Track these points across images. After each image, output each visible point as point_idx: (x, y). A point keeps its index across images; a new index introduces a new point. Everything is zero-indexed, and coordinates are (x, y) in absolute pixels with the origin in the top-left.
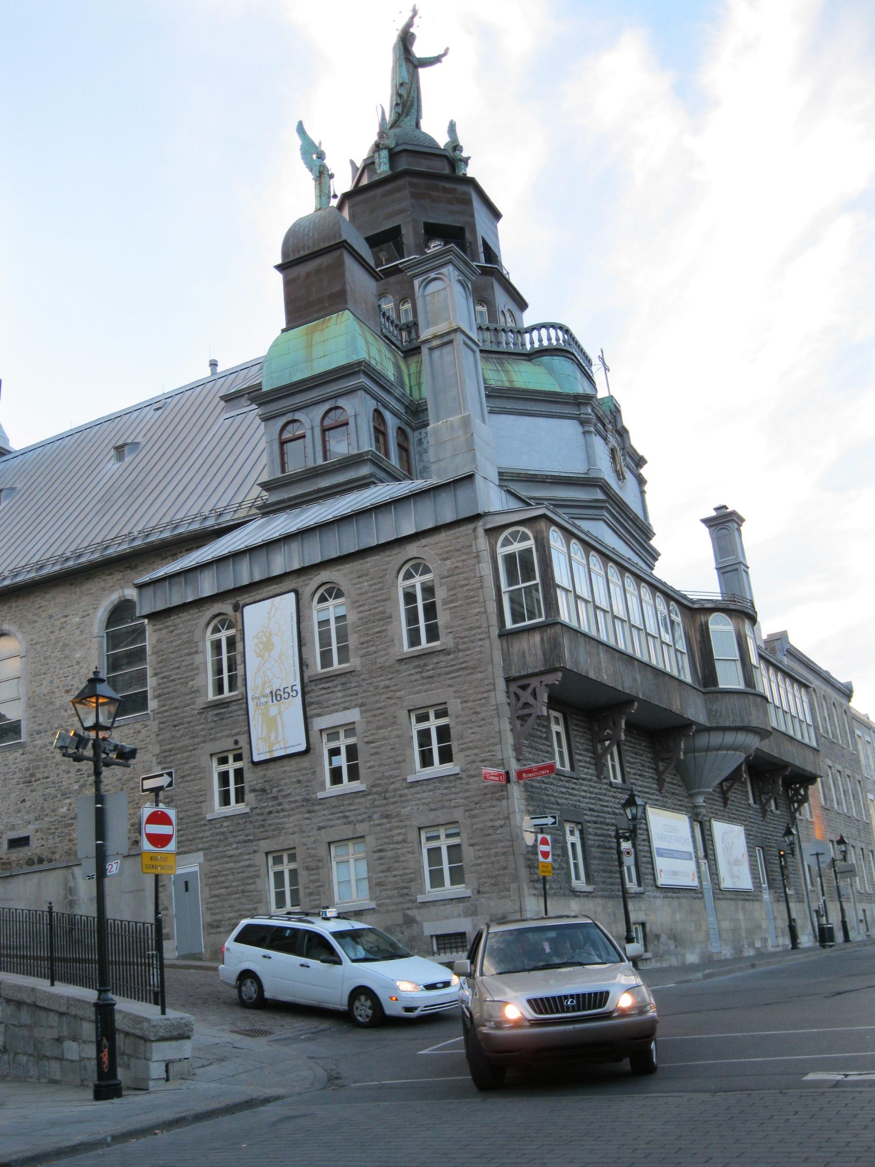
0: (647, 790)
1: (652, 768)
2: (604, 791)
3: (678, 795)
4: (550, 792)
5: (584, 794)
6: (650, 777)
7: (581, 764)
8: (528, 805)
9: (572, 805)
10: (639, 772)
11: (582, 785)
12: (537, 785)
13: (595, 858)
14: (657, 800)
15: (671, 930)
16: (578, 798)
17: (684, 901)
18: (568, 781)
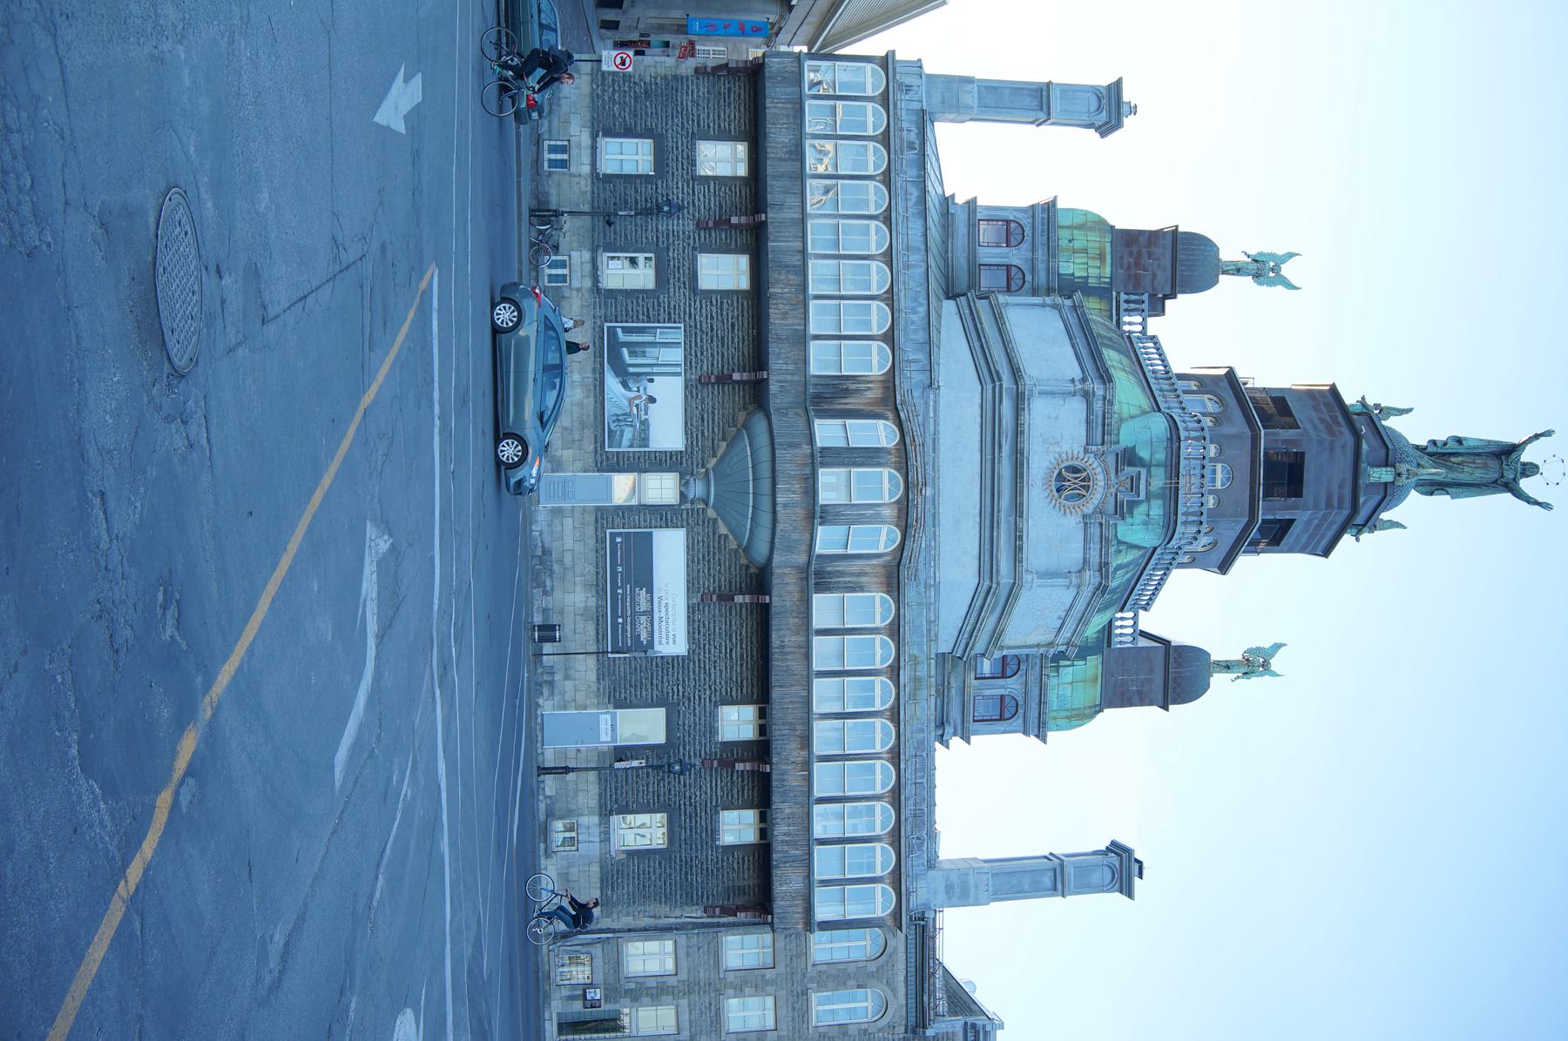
0: (699, 338)
1: (723, 366)
4: (676, 121)
5: (680, 185)
6: (712, 355)
9: (668, 159)
10: (715, 328)
11: (688, 187)
12: (679, 98)
13: (625, 188)
17: (592, 400)
18: (688, 156)
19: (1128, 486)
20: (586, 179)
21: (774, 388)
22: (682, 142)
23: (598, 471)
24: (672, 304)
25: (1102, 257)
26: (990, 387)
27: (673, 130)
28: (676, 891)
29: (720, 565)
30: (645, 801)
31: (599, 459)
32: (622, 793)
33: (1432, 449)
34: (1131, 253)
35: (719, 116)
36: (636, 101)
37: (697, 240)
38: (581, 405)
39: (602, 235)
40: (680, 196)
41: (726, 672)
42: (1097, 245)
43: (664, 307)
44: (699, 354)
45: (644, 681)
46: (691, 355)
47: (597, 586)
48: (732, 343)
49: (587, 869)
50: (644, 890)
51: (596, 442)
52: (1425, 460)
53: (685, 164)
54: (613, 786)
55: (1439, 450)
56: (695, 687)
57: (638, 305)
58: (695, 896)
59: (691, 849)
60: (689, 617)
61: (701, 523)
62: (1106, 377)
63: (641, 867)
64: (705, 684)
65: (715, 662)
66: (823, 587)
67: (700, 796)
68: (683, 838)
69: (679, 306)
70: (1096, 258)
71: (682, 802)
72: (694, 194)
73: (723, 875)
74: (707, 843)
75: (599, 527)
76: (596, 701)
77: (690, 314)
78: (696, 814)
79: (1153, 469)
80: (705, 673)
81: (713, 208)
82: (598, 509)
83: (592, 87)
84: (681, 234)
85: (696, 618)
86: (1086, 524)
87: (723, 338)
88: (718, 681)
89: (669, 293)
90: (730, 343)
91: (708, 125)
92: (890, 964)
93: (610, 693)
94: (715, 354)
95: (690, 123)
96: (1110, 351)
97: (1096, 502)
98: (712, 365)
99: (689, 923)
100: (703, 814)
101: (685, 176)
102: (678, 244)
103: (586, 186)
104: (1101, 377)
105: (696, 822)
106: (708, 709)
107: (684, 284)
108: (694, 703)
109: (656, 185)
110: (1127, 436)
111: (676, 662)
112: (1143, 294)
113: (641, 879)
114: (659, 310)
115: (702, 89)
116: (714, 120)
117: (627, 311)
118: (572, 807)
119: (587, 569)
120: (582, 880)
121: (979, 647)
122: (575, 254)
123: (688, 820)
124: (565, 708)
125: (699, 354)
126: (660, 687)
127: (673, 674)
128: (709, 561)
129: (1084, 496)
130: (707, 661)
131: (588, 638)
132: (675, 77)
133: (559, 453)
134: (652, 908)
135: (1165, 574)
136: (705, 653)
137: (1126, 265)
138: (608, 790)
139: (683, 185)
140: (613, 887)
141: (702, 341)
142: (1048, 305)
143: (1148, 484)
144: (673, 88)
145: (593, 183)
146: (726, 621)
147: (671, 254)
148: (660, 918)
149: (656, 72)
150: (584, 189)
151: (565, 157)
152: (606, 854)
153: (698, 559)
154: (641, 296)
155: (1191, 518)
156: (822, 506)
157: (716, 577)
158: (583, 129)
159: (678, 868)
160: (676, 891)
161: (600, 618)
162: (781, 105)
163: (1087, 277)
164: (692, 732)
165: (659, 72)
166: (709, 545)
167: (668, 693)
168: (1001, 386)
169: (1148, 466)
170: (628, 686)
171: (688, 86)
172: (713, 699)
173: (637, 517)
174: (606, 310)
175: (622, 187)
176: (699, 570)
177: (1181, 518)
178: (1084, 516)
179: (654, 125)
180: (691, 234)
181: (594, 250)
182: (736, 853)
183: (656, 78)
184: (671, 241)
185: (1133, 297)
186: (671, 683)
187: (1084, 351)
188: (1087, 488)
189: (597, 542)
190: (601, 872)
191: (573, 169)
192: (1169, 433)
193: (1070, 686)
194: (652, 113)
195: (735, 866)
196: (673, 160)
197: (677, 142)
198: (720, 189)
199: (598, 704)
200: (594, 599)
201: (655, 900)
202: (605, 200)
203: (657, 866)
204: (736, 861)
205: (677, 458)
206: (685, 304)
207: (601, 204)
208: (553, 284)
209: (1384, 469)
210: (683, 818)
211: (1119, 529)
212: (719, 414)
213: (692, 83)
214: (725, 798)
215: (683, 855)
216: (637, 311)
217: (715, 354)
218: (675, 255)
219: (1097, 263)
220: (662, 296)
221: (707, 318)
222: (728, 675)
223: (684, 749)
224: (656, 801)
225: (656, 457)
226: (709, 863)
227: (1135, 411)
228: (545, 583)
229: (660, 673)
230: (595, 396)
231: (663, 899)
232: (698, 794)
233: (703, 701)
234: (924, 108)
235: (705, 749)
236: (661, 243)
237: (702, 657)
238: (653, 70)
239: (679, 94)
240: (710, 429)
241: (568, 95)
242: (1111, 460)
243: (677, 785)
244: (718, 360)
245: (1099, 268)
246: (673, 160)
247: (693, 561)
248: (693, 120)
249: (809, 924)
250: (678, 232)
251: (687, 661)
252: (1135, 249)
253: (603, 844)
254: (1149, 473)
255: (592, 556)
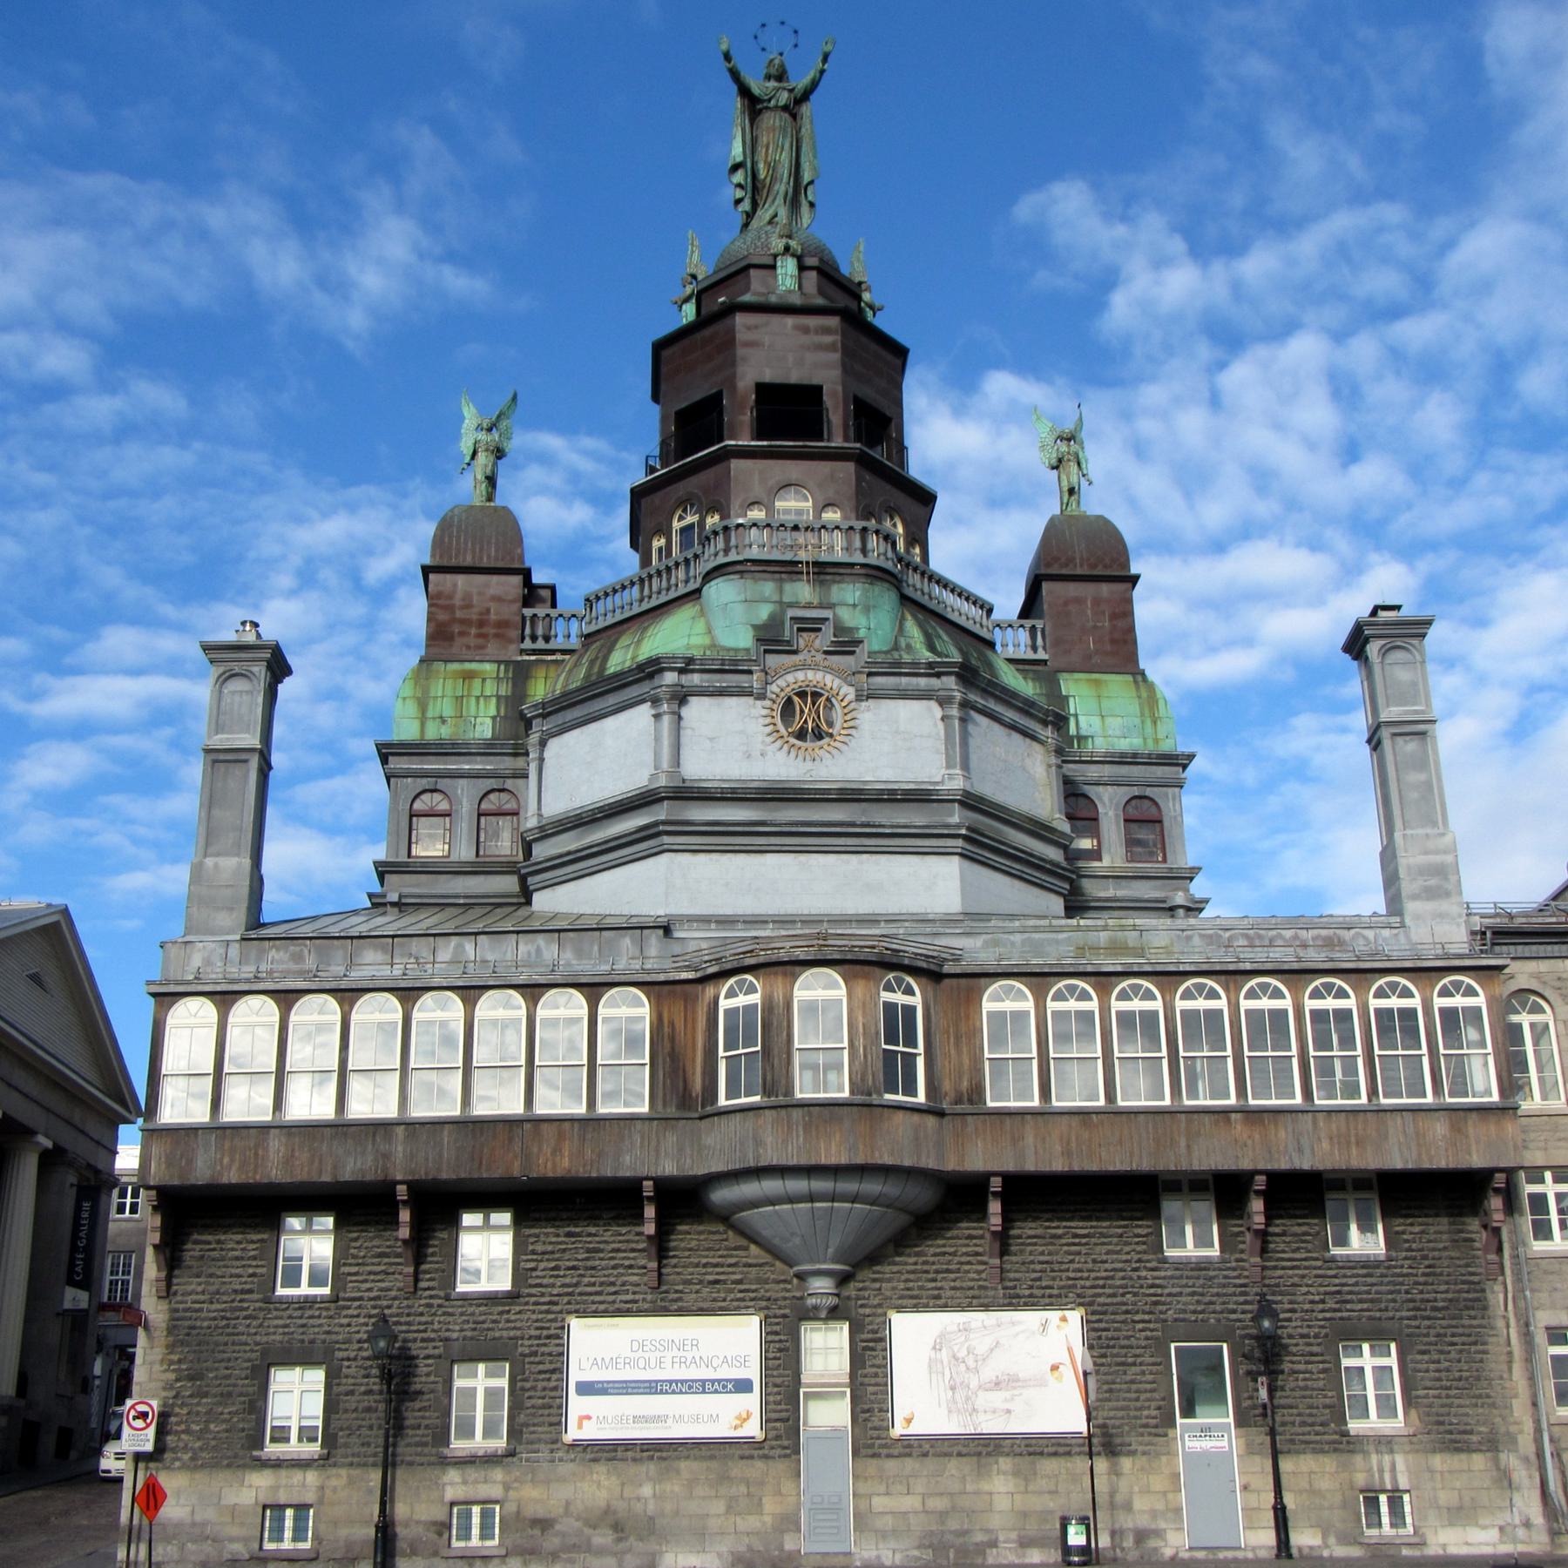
1: (633, 1250)
2: (421, 1309)
3: (740, 1282)
4: (241, 1329)
5: (345, 1321)
6: (614, 1267)
7: (354, 1278)
8: (171, 1353)
9: (302, 1341)
12: (206, 1324)
13: (346, 1411)
14: (636, 1302)
15: (607, 1511)
16: (326, 1328)
17: (683, 1465)
18: (300, 1308)
19: (813, 635)
20: (328, 1477)
21: (668, 1168)
22: (276, 1318)
23: (798, 1453)
24: (533, 1332)
25: (468, 676)
26: (666, 839)
27: (256, 1334)
28: (1463, 1326)
29: (944, 1254)
30: (1322, 1376)
31: (778, 1452)
32: (1311, 1415)
33: (746, 206)
34: (462, 634)
35: (237, 1258)
36: (206, 1395)
37: (432, 1293)
38: (692, 1483)
39: (419, 1449)
40: (362, 1320)
41: (1110, 1243)
42: (449, 683)
43: (538, 1345)
44: (613, 1289)
45: (1128, 1378)
46: (614, 1302)
47: (979, 1454)
48: (595, 1235)
49: (1438, 1476)
50: (1467, 1379)
51: (751, 1457)
52: (764, 215)
53: (310, 1313)
54: (1300, 1430)
55: (749, 195)
56: (1135, 1294)
57: (534, 1388)
58: (1471, 1296)
59: (1394, 1301)
60: (1026, 1304)
61: (877, 1285)
62: (650, 669)
63: (1429, 1384)
64: (1131, 1278)
65: (1094, 1261)
66: (977, 1093)
67: (1307, 1286)
68: (1378, 1314)
69: (537, 1321)
70: (470, 686)
71: (1320, 1316)
72: (360, 1299)
73: (1434, 1249)
74: (1382, 1276)
75: (884, 1451)
76: (1164, 1459)
77: (550, 1303)
78: (1339, 1292)
79: (786, 599)
80: (1112, 1278)
81: (383, 1268)
82: (855, 1453)
83: (179, 1468)
84: (423, 1319)
85: (1027, 1292)
86: (868, 697)
87: (589, 1251)
88: (1124, 1257)
89: (516, 1338)
90: (597, 1239)
91: (251, 1276)
92: (1558, 984)
93: (1150, 1434)
94: (612, 1263)
95: (246, 1305)
96: (609, 663)
97: (837, 682)
98: (631, 1267)
99: (1515, 1306)
100: (1337, 1281)
101: (331, 1313)
102: (439, 1322)
103: (339, 1476)
104: (651, 676)
105: (1350, 1293)
106: (1169, 1273)
107: (501, 1313)
108: (1161, 1295)
109: (343, 1360)
110: (740, 638)
111: (1096, 1325)
112: (524, 618)
113: (1449, 1384)
114: (543, 1354)
115: (193, 1287)
116: (244, 1266)
117: (544, 1407)
118: (1338, 1498)
119: (953, 1472)
120: (1458, 1484)
121: (1053, 854)
122: (450, 1494)
123: (1348, 1306)
124: (1178, 1510)
125: (613, 1289)
126: (1138, 1351)
127: (1116, 1330)
128: (937, 1272)
129: (828, 699)
130: (1093, 1275)
131: (1063, 1471)
132: (171, 1330)
133: (768, 1519)
134: (1495, 1365)
135: (938, 582)
136: (1081, 1278)
137: (480, 641)
138: (1307, 1438)
139: (346, 1316)
140: (1465, 1432)
141: (594, 1284)
142: (542, 752)
143: (809, 606)
144: (188, 1335)
145: (335, 1465)
146: (1030, 1244)
147: (455, 1335)
148: (1510, 1353)
149: (162, 1361)
150: (344, 1481)
151: (289, 1513)
152: (1411, 1443)
153: (932, 1289)
154: (519, 1384)
155: (858, 544)
156: (852, 1092)
157: (964, 1259)
158: (246, 1483)
159: (1427, 1323)
160: (1463, 1326)
161: (1031, 1449)
162: (226, 1160)
163: (498, 697)
164: (1207, 1299)
165: (160, 1357)
166: (913, 1272)
167: (1147, 1338)
168: (664, 823)
169: (783, 605)
170: (1139, 1404)
171: (186, 1310)
172: (1154, 1264)
173: (870, 1389)
174: (539, 1441)
175: (344, 1416)
176: (953, 1288)
177: (858, 558)
178: (859, 698)
179: (246, 1365)
180: (423, 1302)
181: (445, 1462)
182: (1397, 1229)
183: (171, 1363)
184: (433, 1335)
185: (528, 631)
186: (1130, 1333)
187: (612, 700)
188: (816, 695)
189: (910, 1455)
190: (1441, 1451)
191: (310, 1497)
192: (732, 577)
193: (1109, 720)
194: (227, 1368)
195: (1417, 1229)
196: (303, 1333)
197: (276, 1327)
198: (354, 1257)
199: (1168, 1453)
200: (1001, 1460)
201: (1481, 1361)
202: (363, 1445)
203: (1426, 1357)
204: (1410, 1228)
205: (777, 1324)
206: (534, 1312)
207: (371, 1450)
208: (497, 1531)
209: (779, 271)
210: (1345, 1314)
211: (876, 648)
212: (707, 1257)
213: (182, 1302)
214: (1310, 1246)
215: (1405, 1314)
216: (544, 1389)
217: (612, 1263)
218: (457, 1328)
219: (477, 683)
220: (520, 1350)
221: (558, 1276)
222: (1115, 1240)
223: (1234, 1312)
224: (1320, 1358)
225: (775, 1358)
226: (1414, 1271)
227: (700, 626)
228: (977, 1544)
229: (1115, 1351)
230: (679, 1458)
231: (1480, 1347)
232: (1305, 1289)
233: (1157, 1282)
234: (238, 937)
235: (1235, 1278)
236: (437, 1352)
237: (1088, 1283)
238: (157, 1367)
239: (198, 1323)
240: (730, 1270)
241: (188, 1509)
242: (773, 661)
243: (1294, 1324)
244: (624, 1258)
245: (484, 680)
246: (303, 1333)
247: (938, 1297)
248: (241, 1301)
249: (1506, 1110)
250: (419, 1324)
251: (1096, 1308)
252: (456, 629)
253: (1396, 1447)
254: (791, 605)
255: (931, 1464)
